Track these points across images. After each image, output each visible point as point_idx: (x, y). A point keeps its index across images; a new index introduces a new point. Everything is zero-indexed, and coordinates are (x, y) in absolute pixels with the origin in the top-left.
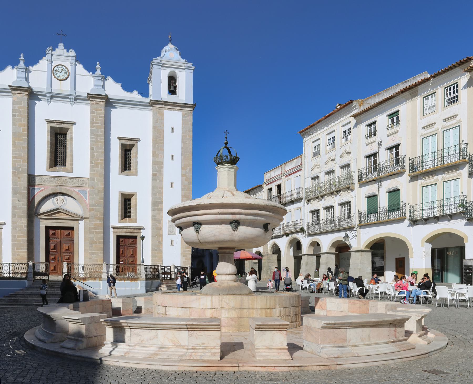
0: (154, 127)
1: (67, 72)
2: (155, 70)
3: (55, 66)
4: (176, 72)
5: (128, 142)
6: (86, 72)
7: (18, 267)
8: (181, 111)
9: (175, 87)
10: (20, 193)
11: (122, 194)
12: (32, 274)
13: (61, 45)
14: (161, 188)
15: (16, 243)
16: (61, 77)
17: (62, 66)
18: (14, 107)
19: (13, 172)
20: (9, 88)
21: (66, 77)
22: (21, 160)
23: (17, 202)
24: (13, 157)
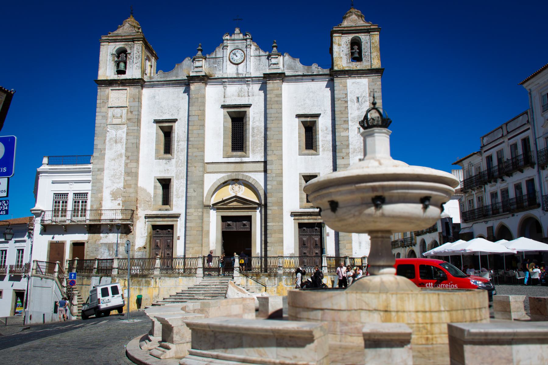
1: (244, 55)
2: (337, 38)
3: (232, 51)
4: (360, 37)
5: (309, 119)
6: (262, 53)
7: (194, 262)
8: (366, 78)
9: (360, 53)
11: (303, 176)
12: (201, 269)
13: (237, 31)
16: (237, 61)
17: (238, 50)
20: (186, 78)
21: (242, 60)
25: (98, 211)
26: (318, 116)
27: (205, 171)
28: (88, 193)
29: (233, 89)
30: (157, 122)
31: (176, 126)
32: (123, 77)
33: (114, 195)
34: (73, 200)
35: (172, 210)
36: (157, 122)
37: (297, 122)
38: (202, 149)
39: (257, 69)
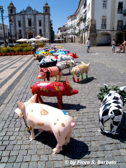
0: (44, 18)
14: (45, 28)
26: (41, 20)
27: (26, 29)
29: (29, 16)
30: (18, 21)
31: (21, 22)
32: (12, 14)
33: (13, 33)
36: (18, 21)
37: (38, 21)
38: (25, 26)
39: (32, 13)
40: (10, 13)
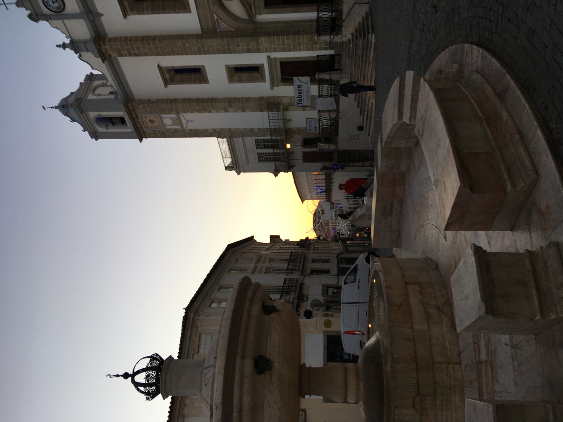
10: (228, 45)
15: (292, 47)
18: (125, 55)
19: (205, 53)
22: (187, 45)
23: (240, 48)
24: (187, 54)
25: (272, 131)
28: (255, 139)
34: (263, 149)
35: (263, 64)
40: (129, 128)
